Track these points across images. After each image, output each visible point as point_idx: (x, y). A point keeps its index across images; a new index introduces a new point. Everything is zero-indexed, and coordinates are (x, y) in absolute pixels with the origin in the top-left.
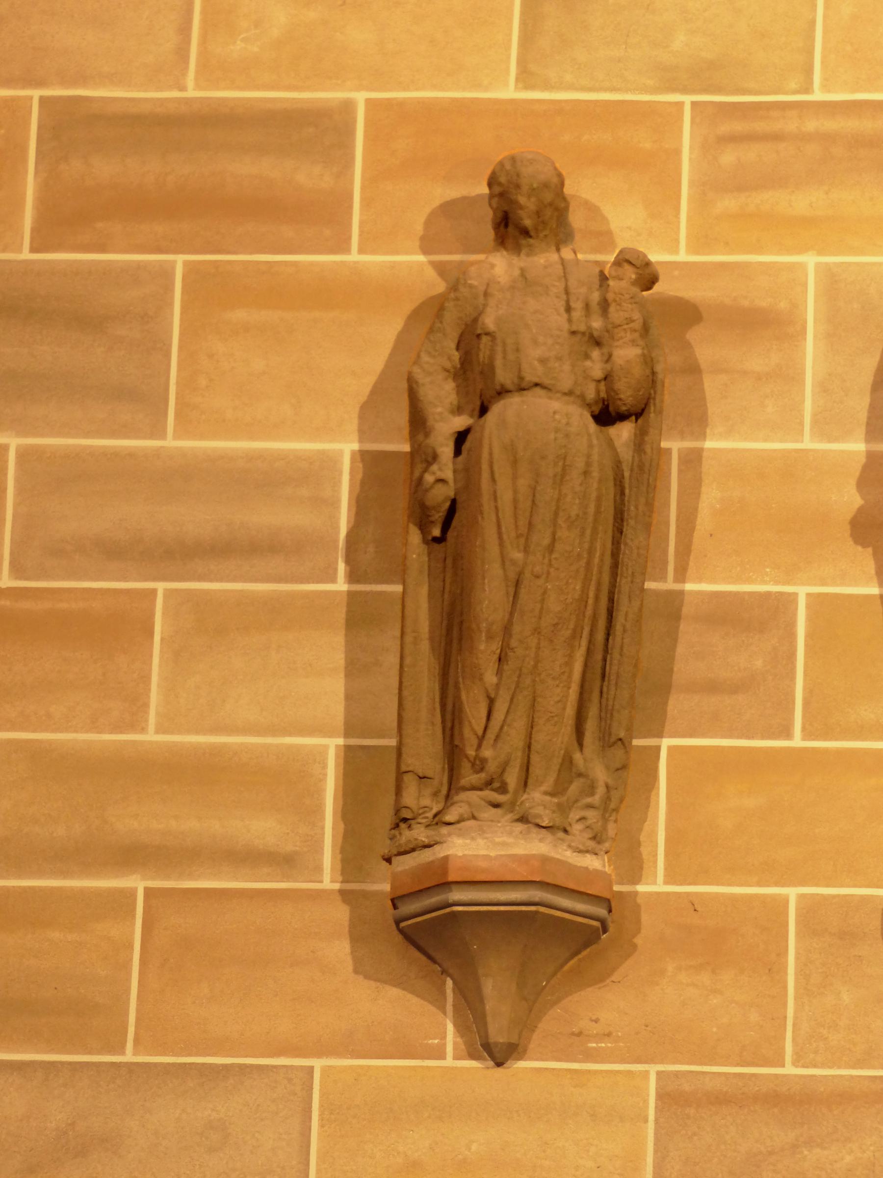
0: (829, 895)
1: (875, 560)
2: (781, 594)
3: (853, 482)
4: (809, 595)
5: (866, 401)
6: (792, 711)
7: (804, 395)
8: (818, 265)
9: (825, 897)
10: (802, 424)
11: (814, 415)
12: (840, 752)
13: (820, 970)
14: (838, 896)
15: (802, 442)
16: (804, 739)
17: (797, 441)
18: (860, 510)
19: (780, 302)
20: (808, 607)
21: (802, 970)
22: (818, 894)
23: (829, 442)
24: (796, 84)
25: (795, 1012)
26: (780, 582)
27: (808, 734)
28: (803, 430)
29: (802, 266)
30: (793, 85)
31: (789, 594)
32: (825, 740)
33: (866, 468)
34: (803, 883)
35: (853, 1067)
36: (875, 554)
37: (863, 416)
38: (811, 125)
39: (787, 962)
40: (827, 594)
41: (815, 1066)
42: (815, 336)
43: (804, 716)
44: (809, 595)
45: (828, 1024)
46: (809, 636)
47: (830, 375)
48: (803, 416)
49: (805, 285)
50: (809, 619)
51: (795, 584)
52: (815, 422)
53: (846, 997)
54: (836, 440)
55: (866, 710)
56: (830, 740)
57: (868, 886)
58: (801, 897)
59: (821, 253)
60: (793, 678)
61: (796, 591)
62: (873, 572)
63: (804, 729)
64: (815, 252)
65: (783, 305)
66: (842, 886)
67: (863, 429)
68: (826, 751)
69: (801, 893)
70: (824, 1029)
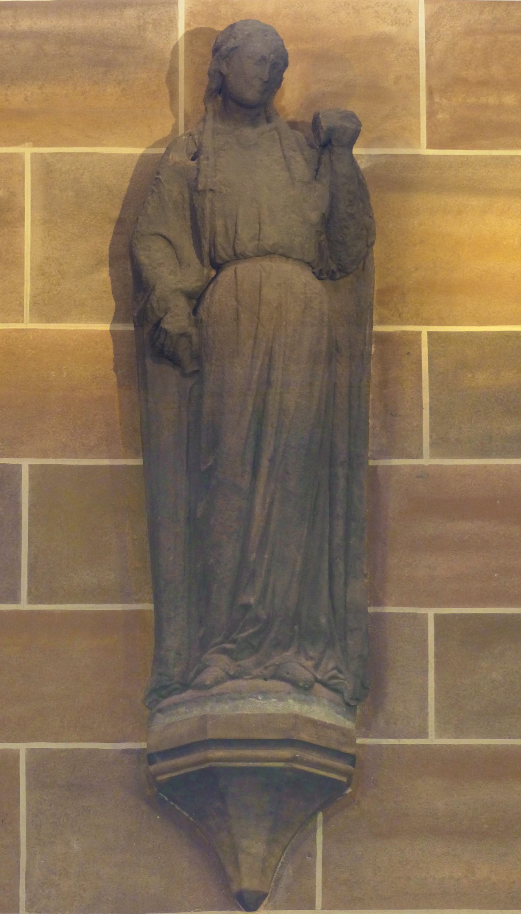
4: (31, 466)
8: (34, 156)
10: (21, 305)
11: (33, 297)
12: (63, 614)
15: (23, 322)
16: (30, 602)
17: (17, 322)
20: (31, 477)
22: (47, 749)
23: (48, 322)
25: (28, 861)
27: (33, 598)
28: (23, 311)
29: (20, 157)
32: (50, 603)
39: (19, 812)
40: (49, 466)
42: (32, 222)
43: (29, 580)
44: (31, 466)
45: (59, 871)
46: (32, 506)
47: (47, 259)
48: (22, 298)
49: (22, 174)
50: (32, 490)
51: (18, 457)
52: (34, 303)
55: (88, 575)
56: (55, 603)
57: (94, 741)
58: (31, 752)
59: (36, 144)
60: (18, 546)
61: (20, 463)
63: (29, 593)
64: (31, 143)
69: (32, 747)
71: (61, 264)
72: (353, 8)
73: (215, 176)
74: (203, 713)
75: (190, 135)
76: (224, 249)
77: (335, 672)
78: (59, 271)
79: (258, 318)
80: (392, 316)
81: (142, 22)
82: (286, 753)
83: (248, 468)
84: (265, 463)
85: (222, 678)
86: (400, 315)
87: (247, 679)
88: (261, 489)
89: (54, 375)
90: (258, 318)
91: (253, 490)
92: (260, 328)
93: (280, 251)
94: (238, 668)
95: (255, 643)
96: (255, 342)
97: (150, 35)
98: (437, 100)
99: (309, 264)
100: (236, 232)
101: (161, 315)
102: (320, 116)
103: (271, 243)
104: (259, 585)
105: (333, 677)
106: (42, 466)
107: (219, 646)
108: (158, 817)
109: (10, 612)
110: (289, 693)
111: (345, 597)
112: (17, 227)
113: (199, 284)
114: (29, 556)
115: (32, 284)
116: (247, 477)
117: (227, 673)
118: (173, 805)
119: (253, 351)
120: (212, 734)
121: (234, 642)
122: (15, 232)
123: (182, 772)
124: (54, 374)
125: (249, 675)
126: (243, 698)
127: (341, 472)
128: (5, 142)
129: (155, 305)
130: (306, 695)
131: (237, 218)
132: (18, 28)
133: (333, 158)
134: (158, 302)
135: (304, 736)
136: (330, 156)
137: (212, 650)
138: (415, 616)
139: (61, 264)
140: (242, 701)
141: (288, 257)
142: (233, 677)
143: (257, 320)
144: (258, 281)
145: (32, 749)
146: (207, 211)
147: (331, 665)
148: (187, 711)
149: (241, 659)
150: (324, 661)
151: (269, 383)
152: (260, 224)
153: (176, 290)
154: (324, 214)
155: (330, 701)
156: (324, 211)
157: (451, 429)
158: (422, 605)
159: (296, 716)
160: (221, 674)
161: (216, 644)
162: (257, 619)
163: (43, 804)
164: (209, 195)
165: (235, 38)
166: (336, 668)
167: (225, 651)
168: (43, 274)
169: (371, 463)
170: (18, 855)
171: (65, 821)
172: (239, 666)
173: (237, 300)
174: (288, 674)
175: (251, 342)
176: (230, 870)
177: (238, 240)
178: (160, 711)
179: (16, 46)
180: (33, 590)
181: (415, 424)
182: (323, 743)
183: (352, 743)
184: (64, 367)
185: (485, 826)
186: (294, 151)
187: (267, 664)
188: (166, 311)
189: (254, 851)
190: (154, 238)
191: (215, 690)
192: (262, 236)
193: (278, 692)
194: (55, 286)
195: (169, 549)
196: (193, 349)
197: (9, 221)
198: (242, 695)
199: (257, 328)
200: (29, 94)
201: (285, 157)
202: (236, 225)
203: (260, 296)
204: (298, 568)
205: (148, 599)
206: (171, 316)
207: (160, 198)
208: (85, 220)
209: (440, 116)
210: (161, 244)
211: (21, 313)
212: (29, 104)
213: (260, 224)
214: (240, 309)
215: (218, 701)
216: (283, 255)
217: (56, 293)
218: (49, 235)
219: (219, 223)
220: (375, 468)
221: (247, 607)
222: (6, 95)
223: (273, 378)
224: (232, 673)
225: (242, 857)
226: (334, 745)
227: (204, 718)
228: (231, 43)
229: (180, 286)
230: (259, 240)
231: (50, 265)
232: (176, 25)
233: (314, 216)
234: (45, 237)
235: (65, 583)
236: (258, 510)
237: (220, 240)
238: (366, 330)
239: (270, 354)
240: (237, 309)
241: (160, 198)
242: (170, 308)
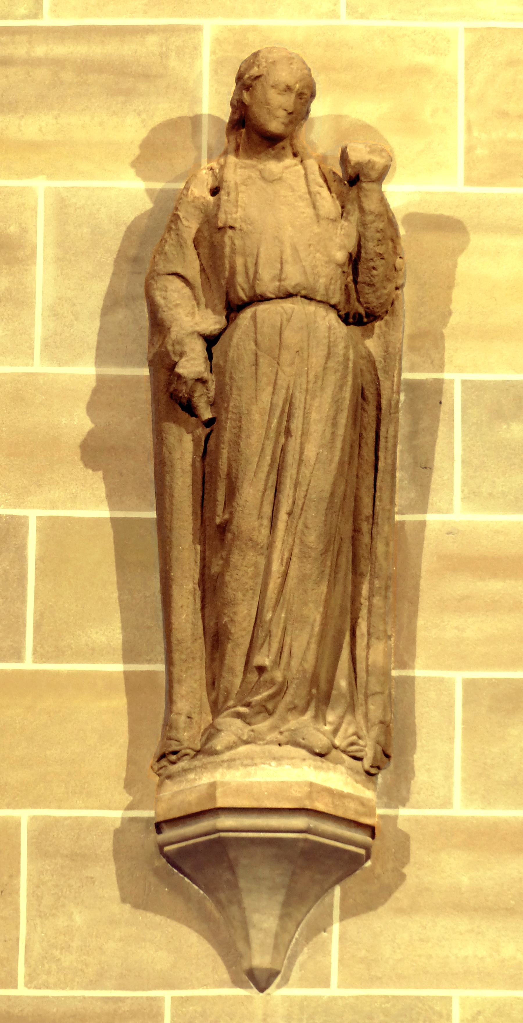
0: (61, 817)
1: (105, 484)
2: (12, 517)
3: (83, 406)
4: (39, 518)
5: (97, 324)
6: (23, 634)
7: (33, 319)
9: (57, 821)
10: (31, 348)
11: (45, 339)
13: (52, 892)
14: (70, 818)
16: (35, 662)
17: (27, 365)
18: (91, 433)
19: (10, 226)
20: (39, 530)
21: (34, 892)
24: (25, 9)
25: (28, 934)
26: (10, 505)
27: (39, 656)
30: (22, 11)
31: (20, 517)
33: (95, 391)
34: (35, 804)
35: (86, 988)
36: (105, 478)
37: (93, 339)
38: (40, 50)
39: (19, 883)
40: (58, 517)
41: (48, 987)
42: (45, 259)
44: (39, 518)
46: (40, 559)
47: (60, 299)
48: (32, 340)
50: (40, 543)
51: (25, 508)
52: (45, 346)
53: (78, 919)
54: (66, 363)
55: (97, 633)
57: (100, 808)
58: (34, 819)
59: (50, 177)
60: (24, 601)
62: (103, 495)
63: (35, 652)
64: (44, 176)
65: (13, 229)
66: (73, 808)
67: (93, 353)
68: (57, 674)
70: (57, 950)
71: (74, 305)
72: (389, 36)
73: (236, 212)
74: (212, 780)
75: (211, 169)
76: (243, 289)
77: (355, 738)
78: (72, 312)
79: (278, 363)
80: (424, 362)
81: (164, 49)
82: (300, 822)
83: (266, 522)
84: (283, 516)
85: (234, 742)
86: (432, 363)
87: (260, 745)
88: (278, 544)
89: (65, 422)
90: (278, 363)
91: (270, 546)
92: (280, 373)
93: (303, 292)
94: (252, 733)
95: (270, 706)
96: (274, 389)
97: (173, 63)
98: (476, 134)
99: (334, 307)
100: (256, 272)
101: (176, 359)
102: (348, 150)
103: (293, 284)
104: (275, 646)
105: (352, 744)
106: (50, 518)
107: (233, 710)
108: (166, 889)
109: (13, 671)
110: (304, 760)
111: (367, 658)
112: (28, 265)
113: (218, 327)
114: (35, 612)
115: (44, 326)
116: (265, 531)
117: (240, 738)
118: (182, 878)
119: (272, 399)
120: (221, 803)
121: (248, 705)
122: (26, 270)
123: (191, 842)
124: (65, 420)
125: (263, 739)
126: (256, 765)
127: (365, 527)
128: (17, 175)
129: (170, 348)
130: (323, 762)
131: (257, 257)
132: (33, 54)
133: (361, 194)
134: (173, 345)
135: (320, 806)
136: (358, 193)
137: (225, 713)
138: (441, 681)
139: (74, 305)
140: (253, 768)
141: (311, 299)
142: (247, 742)
143: (276, 365)
144: (279, 324)
145: (34, 816)
146: (227, 250)
147: (351, 730)
148: (197, 777)
149: (255, 724)
150: (344, 726)
151: (288, 432)
152: (282, 263)
153: (193, 333)
154: (350, 254)
155: (350, 769)
156: (350, 251)
157: (484, 482)
158: (449, 667)
159: (311, 784)
160: (234, 738)
161: (229, 708)
162: (272, 682)
163: (44, 874)
164: (230, 232)
165: (258, 66)
166: (356, 734)
167: (239, 715)
168: (55, 315)
169: (398, 518)
170: (17, 927)
171: (68, 892)
172: (253, 731)
173: (256, 344)
174: (303, 739)
175: (270, 389)
176: (241, 945)
177: (258, 280)
178: (169, 777)
179: (31, 74)
180: (38, 649)
181: (446, 477)
182: (340, 813)
183: (372, 813)
184: (76, 414)
185: (513, 902)
186: (321, 187)
187: (282, 730)
188: (182, 355)
189: (265, 925)
190: (171, 277)
191: (226, 756)
192: (283, 276)
193: (293, 758)
194: (68, 328)
195: (182, 607)
196: (209, 395)
197: (20, 259)
198: (254, 762)
199: (277, 374)
200: (43, 124)
201: (310, 193)
202: (256, 264)
203: (280, 341)
204: (317, 629)
205: (160, 659)
206: (187, 361)
207: (178, 235)
208: (101, 258)
209: (480, 152)
210: (178, 283)
211: (31, 356)
212: (44, 135)
213: (282, 263)
214: (259, 353)
215: (229, 767)
216: (305, 297)
217: (68, 335)
218: (62, 274)
219: (239, 261)
220: (402, 523)
221: (261, 669)
222: (19, 125)
223: (293, 426)
224: (245, 738)
225: (253, 933)
226: (351, 816)
227: (213, 786)
228: (255, 71)
229: (198, 329)
230: (280, 280)
231: (63, 306)
232: (200, 52)
233: (341, 256)
234: (58, 276)
235: (73, 642)
236: (276, 567)
237: (240, 279)
238: (394, 376)
239: (290, 402)
240: (256, 354)
241: (178, 235)
242: (186, 352)
